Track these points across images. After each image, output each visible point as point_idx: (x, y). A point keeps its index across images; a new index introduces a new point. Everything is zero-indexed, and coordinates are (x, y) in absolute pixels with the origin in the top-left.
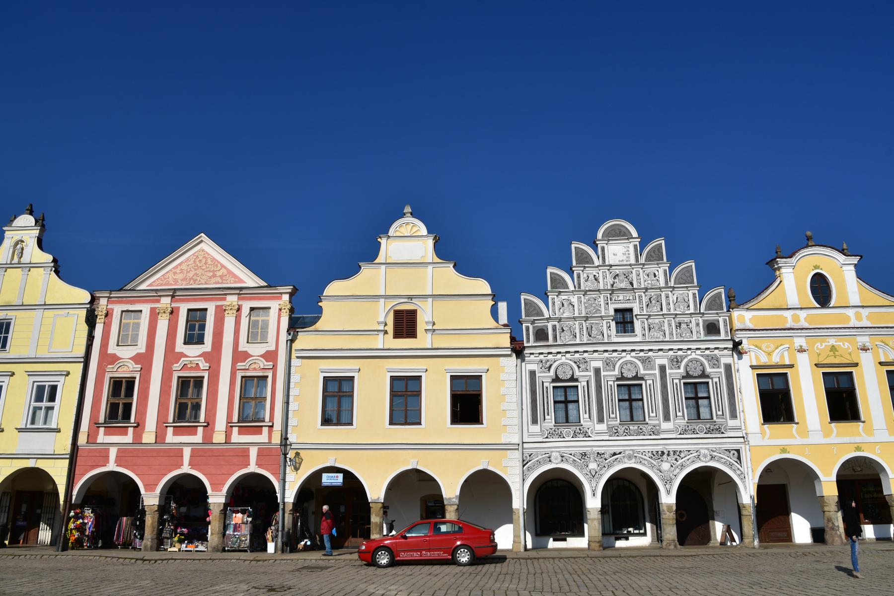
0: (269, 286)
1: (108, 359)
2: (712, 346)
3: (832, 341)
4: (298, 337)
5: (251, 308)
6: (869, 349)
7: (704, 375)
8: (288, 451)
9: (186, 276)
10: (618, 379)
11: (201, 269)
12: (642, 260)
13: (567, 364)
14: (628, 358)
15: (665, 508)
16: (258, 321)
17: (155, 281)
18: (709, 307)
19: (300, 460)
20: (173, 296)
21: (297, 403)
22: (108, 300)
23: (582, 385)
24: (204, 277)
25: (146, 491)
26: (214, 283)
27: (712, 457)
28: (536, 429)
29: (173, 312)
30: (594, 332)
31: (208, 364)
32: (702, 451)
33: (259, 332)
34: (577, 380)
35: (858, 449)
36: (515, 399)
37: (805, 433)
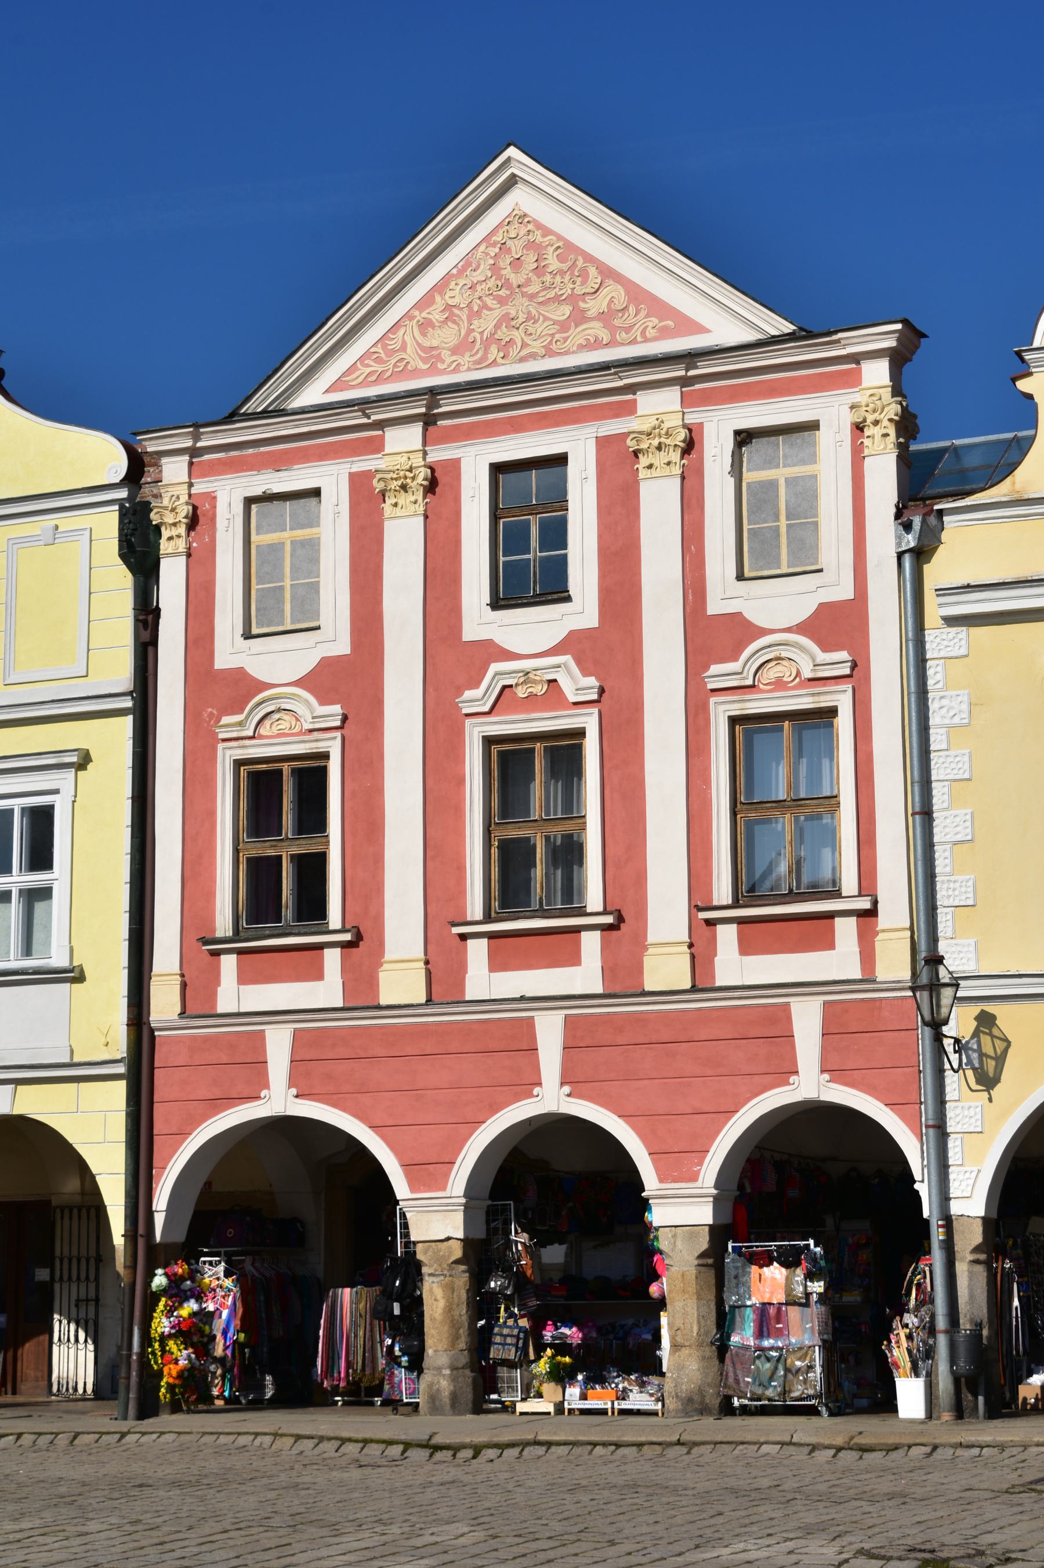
0: (803, 334)
4: (944, 536)
5: (737, 433)
8: (944, 1011)
9: (470, 331)
11: (524, 294)
16: (773, 485)
17: (353, 368)
19: (1000, 1045)
20: (429, 421)
21: (963, 813)
22: (191, 464)
24: (540, 328)
25: (413, 1189)
26: (581, 347)
31: (592, 681)
33: (783, 530)
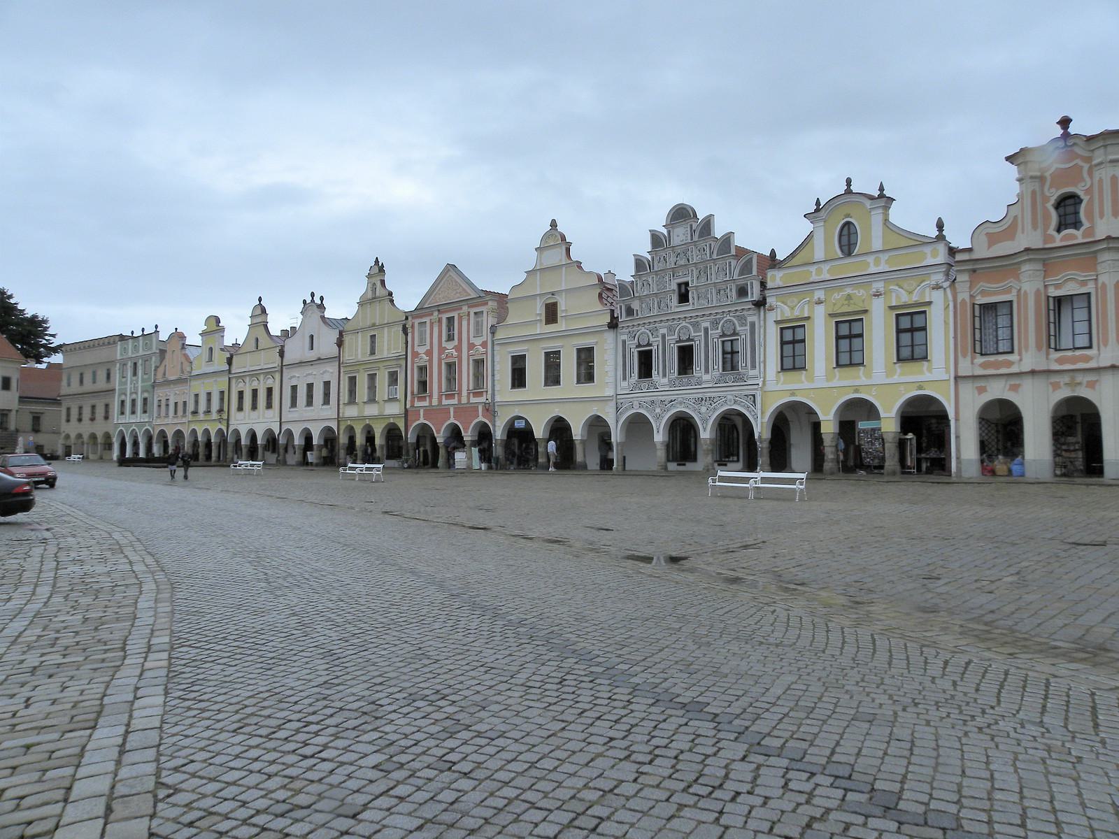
1: (416, 355)
2: (739, 308)
3: (849, 291)
6: (881, 295)
7: (735, 334)
10: (677, 342)
12: (696, 238)
13: (645, 333)
14: (684, 324)
15: (702, 442)
18: (741, 273)
20: (439, 310)
23: (654, 348)
27: (735, 402)
28: (625, 384)
29: (440, 321)
30: (662, 305)
32: (729, 397)
34: (651, 345)
35: (856, 391)
36: (611, 363)
37: (811, 379)
